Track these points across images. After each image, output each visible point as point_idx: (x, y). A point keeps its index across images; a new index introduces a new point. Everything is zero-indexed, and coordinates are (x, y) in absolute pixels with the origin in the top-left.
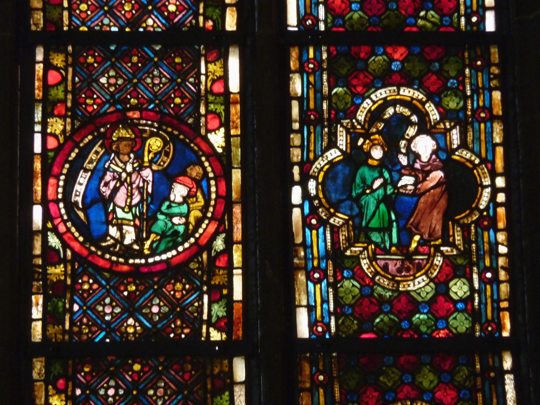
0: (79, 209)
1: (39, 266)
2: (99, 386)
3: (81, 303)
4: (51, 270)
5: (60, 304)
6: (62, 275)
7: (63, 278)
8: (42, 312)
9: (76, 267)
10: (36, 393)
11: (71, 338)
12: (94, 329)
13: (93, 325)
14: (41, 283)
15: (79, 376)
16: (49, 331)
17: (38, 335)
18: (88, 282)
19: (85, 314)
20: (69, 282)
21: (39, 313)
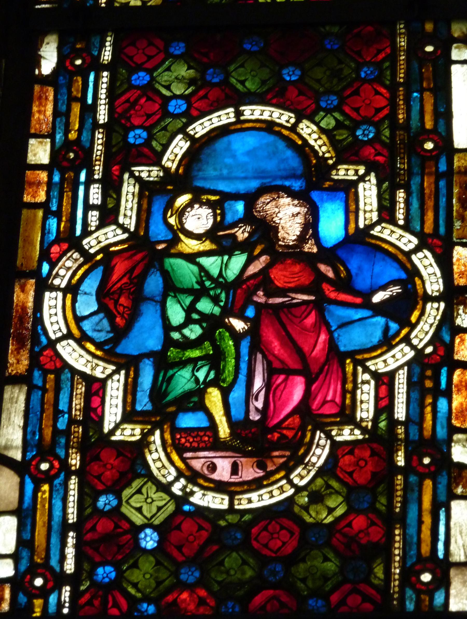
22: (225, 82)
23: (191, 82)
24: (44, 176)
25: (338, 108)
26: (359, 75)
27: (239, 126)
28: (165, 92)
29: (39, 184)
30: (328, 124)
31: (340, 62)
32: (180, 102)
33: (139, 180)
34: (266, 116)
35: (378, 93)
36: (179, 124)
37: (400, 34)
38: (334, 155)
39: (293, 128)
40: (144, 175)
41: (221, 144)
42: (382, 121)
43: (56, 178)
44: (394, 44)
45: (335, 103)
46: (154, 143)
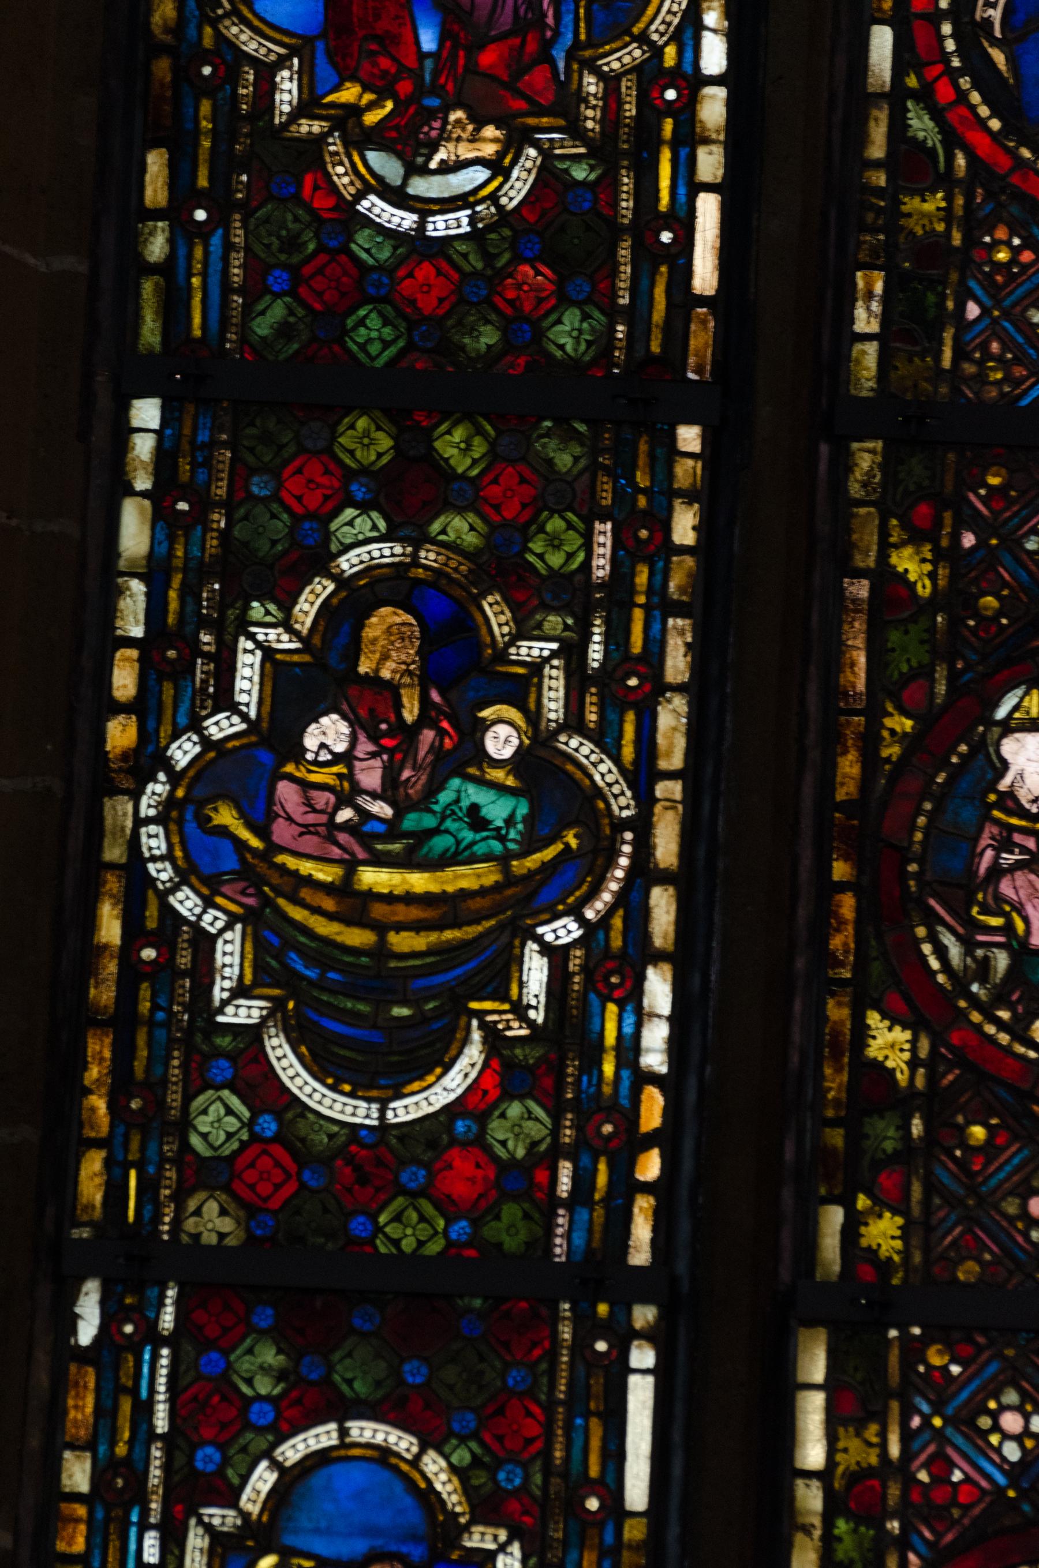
0: (995, 42)
1: (879, 192)
2: (1026, 528)
3: (985, 299)
4: (912, 204)
5: (931, 298)
6: (941, 220)
7: (940, 227)
8: (880, 317)
9: (979, 200)
10: (855, 537)
11: (956, 391)
12: (1019, 371)
13: (1017, 361)
14: (882, 237)
15: (972, 497)
16: (896, 368)
17: (868, 380)
18: (1008, 244)
19: (995, 330)
20: (957, 239)
21: (872, 319)
22: (327, 1381)
23: (281, 1376)
24: (81, 1511)
25: (475, 1436)
26: (504, 1381)
27: (342, 1453)
28: (245, 1389)
29: (77, 1520)
30: (461, 1459)
31: (482, 1359)
32: (267, 1407)
33: (209, 1528)
34: (379, 1438)
35: (529, 1414)
36: (264, 1446)
37: (565, 1318)
38: (467, 1510)
39: (415, 1462)
40: (216, 1521)
41: (318, 1479)
42: (533, 1460)
43: (100, 1514)
44: (555, 1333)
45: (473, 1425)
46: (230, 1472)
